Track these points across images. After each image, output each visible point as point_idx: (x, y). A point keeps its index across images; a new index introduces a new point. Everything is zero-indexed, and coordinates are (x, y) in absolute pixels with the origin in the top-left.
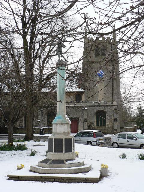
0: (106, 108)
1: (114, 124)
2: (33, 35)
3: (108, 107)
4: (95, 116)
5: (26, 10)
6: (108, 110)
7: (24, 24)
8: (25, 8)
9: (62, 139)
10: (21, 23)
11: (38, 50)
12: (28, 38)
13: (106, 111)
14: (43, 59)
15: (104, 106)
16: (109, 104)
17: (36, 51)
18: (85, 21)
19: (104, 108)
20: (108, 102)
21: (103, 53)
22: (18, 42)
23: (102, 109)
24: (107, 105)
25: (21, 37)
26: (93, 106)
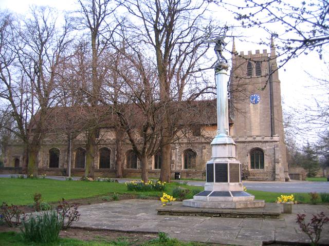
0: (264, 145)
1: (275, 166)
2: (169, 47)
3: (267, 144)
4: (249, 156)
5: (160, 14)
6: (266, 148)
7: (158, 32)
8: (159, 10)
9: (217, 181)
10: (154, 31)
11: (175, 65)
12: (163, 49)
13: (264, 149)
14: (182, 77)
15: (260, 142)
16: (268, 139)
17: (171, 67)
18: (189, 43)
19: (261, 144)
20: (257, 136)
21: (256, 75)
22: (149, 54)
23: (259, 147)
24: (264, 140)
25: (153, 47)
26: (246, 142)
